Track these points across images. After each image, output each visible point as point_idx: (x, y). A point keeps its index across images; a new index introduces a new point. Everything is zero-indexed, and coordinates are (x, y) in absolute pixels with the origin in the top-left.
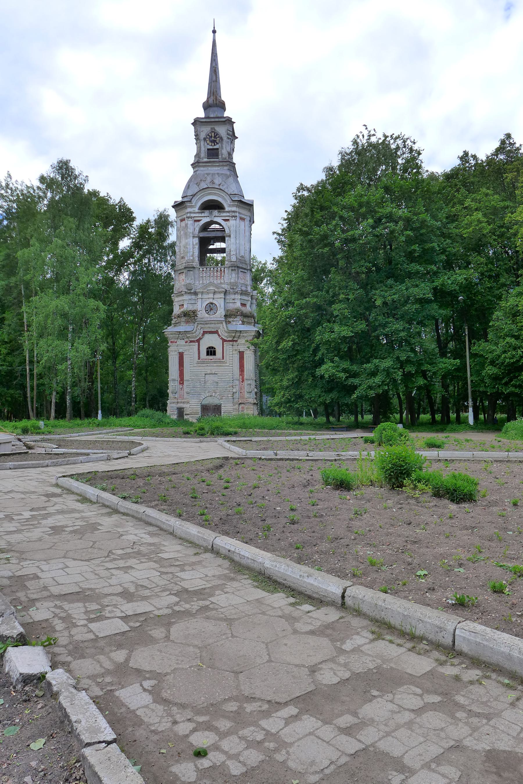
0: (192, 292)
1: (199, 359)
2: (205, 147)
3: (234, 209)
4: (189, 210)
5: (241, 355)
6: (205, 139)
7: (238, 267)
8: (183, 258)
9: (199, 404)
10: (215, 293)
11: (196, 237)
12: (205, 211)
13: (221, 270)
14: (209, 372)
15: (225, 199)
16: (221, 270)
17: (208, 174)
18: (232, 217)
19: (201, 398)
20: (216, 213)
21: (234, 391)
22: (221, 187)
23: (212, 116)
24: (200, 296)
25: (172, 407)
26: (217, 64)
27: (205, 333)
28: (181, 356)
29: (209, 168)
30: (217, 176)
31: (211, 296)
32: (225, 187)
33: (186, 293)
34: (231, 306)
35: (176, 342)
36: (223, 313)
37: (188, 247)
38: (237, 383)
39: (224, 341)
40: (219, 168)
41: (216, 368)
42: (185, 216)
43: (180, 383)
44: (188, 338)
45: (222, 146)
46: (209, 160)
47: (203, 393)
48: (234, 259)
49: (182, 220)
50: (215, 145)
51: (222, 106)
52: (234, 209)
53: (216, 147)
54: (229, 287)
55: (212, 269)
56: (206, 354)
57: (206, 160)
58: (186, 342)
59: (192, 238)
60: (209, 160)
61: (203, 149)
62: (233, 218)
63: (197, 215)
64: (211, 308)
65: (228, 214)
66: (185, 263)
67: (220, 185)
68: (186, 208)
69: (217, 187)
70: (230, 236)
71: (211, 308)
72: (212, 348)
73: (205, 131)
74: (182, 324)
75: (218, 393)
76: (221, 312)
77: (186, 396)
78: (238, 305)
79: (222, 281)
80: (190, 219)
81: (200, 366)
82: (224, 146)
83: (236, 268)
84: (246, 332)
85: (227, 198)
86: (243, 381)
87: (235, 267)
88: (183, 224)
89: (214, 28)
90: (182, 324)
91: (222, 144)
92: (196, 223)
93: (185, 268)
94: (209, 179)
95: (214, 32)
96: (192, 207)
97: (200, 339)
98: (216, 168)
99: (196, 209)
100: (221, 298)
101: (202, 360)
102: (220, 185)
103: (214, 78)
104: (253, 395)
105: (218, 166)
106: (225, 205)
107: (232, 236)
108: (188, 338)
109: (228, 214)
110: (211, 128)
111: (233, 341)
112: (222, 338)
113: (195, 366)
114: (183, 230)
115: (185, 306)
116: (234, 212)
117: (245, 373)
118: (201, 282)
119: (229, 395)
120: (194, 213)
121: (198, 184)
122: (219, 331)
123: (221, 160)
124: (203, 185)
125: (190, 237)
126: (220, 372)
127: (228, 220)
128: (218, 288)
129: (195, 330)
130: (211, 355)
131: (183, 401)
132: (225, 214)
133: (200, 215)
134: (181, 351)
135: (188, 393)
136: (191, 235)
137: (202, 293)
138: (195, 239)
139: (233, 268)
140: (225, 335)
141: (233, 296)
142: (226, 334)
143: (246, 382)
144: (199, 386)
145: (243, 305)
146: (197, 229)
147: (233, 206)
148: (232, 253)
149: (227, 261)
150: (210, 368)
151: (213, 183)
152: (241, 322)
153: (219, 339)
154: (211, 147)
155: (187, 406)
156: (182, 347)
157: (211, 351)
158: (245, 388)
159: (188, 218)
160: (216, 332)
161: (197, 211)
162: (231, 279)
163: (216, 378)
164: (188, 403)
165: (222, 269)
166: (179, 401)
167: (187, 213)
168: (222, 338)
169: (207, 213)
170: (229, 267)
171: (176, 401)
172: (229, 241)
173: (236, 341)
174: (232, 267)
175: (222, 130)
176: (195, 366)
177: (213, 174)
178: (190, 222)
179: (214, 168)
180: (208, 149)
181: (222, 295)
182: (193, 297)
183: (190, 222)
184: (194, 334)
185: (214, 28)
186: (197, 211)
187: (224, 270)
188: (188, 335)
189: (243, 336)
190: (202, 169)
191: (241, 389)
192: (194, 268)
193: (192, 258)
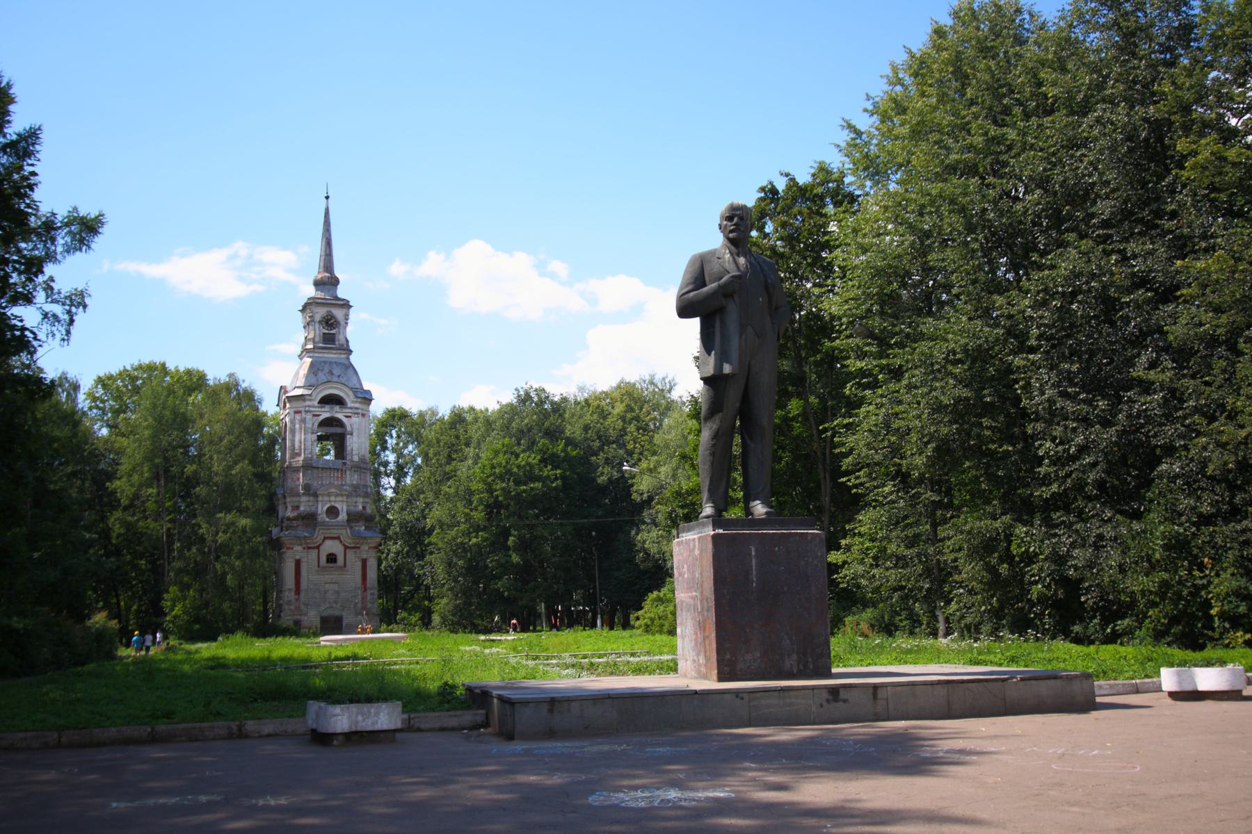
1: (319, 566)
2: (320, 330)
3: (357, 405)
4: (308, 403)
5: (364, 562)
7: (361, 468)
10: (337, 495)
15: (348, 395)
17: (325, 362)
18: (355, 414)
20: (337, 408)
24: (320, 498)
26: (330, 235)
27: (325, 538)
28: (298, 563)
29: (326, 355)
30: (335, 366)
31: (332, 498)
32: (345, 379)
34: (352, 508)
38: (360, 592)
39: (346, 547)
42: (302, 409)
44: (307, 544)
49: (295, 412)
52: (357, 405)
57: (321, 345)
58: (304, 548)
63: (317, 409)
64: (333, 511)
65: (350, 411)
67: (339, 376)
68: (304, 400)
69: (335, 379)
70: (352, 434)
71: (333, 511)
72: (333, 554)
73: (320, 312)
76: (343, 516)
77: (303, 607)
82: (341, 331)
85: (351, 393)
86: (365, 590)
88: (298, 417)
90: (300, 528)
93: (303, 466)
94: (326, 370)
95: (327, 198)
96: (311, 400)
97: (320, 545)
99: (316, 403)
102: (339, 376)
103: (328, 252)
106: (347, 400)
112: (344, 545)
115: (302, 509)
116: (357, 408)
120: (314, 407)
121: (315, 374)
127: (350, 417)
130: (331, 562)
132: (347, 410)
134: (298, 557)
136: (310, 431)
137: (323, 495)
140: (349, 542)
141: (355, 499)
142: (350, 541)
143: (369, 592)
145: (364, 508)
146: (316, 424)
147: (356, 402)
148: (354, 453)
151: (332, 374)
154: (327, 332)
157: (332, 558)
158: (369, 598)
159: (306, 412)
160: (338, 538)
163: (336, 587)
168: (344, 545)
169: (327, 408)
173: (359, 548)
175: (338, 313)
177: (331, 363)
178: (309, 416)
180: (324, 334)
181: (345, 499)
182: (312, 498)
183: (309, 416)
190: (316, 355)
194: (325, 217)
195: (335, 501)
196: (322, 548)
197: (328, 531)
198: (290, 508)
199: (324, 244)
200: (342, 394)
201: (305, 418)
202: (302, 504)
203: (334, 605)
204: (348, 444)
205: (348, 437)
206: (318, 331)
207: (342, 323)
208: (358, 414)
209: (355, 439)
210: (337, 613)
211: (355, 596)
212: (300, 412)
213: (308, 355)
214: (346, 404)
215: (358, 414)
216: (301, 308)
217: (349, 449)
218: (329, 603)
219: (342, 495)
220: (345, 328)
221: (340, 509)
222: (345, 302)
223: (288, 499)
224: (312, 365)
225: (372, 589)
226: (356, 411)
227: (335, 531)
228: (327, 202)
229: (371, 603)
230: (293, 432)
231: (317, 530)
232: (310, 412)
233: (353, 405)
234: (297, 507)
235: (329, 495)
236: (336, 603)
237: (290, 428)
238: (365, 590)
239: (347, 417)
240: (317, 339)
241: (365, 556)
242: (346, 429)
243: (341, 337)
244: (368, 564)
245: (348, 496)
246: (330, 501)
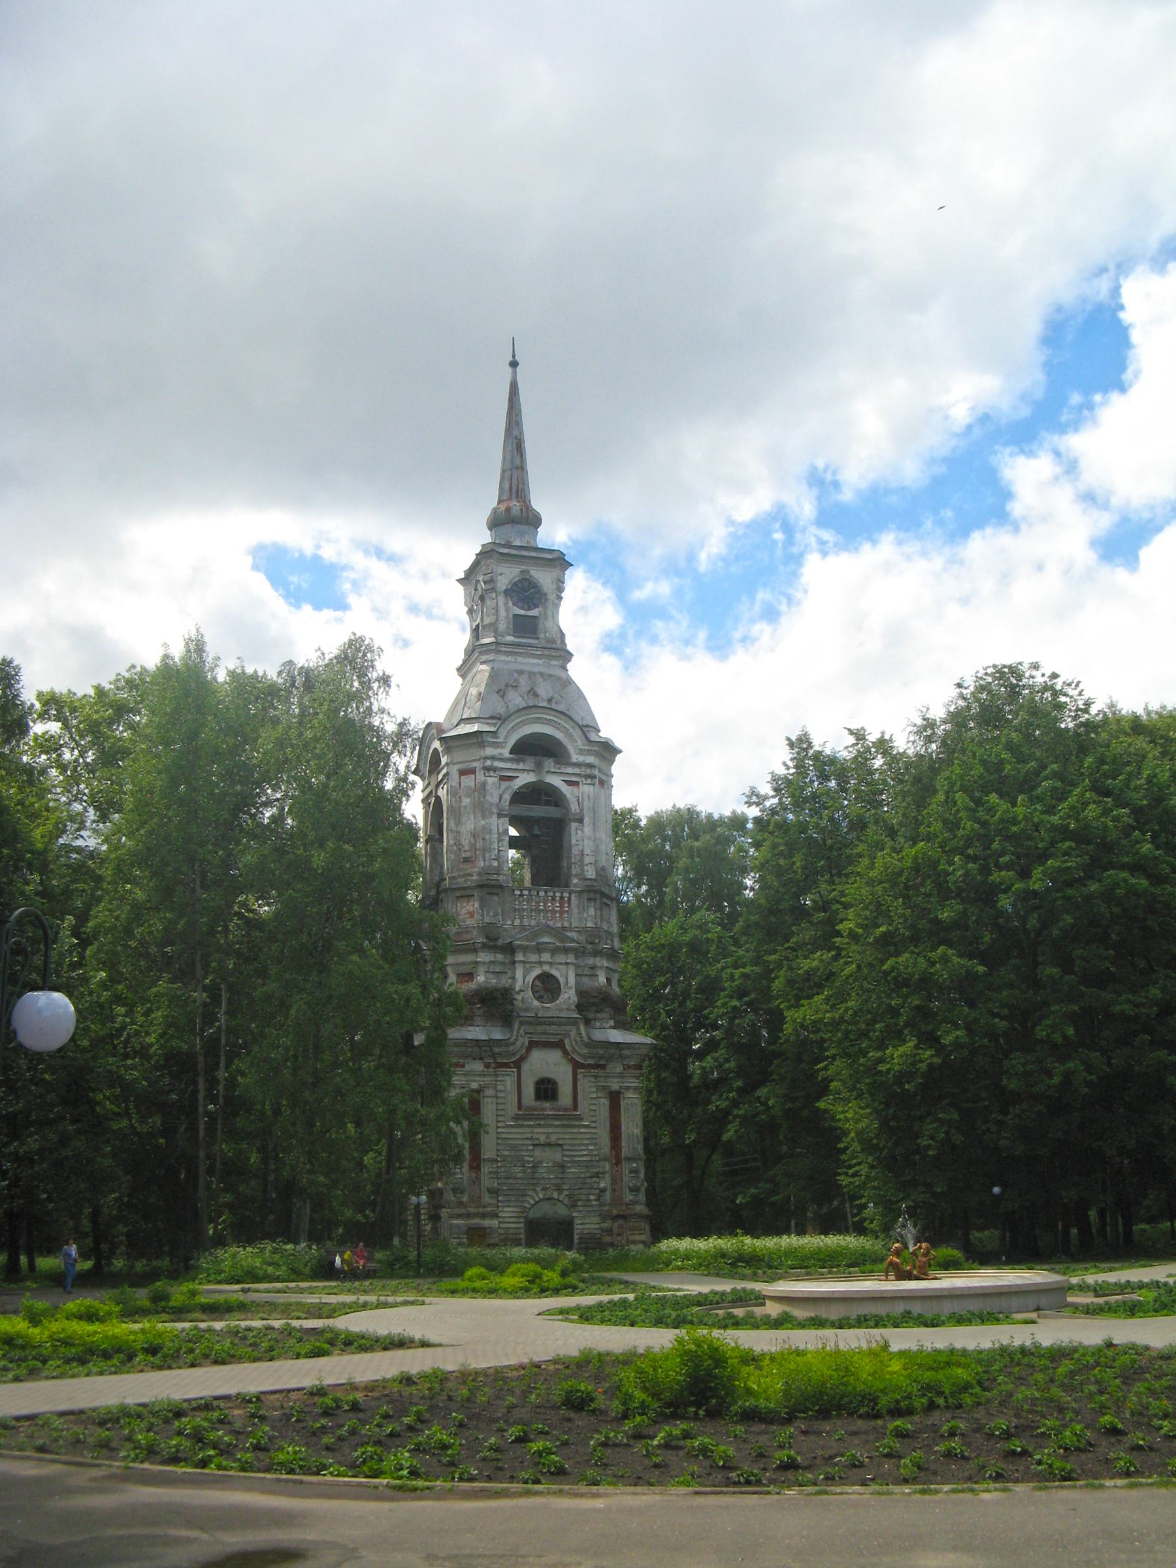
0: (494, 941)
1: (520, 1107)
2: (507, 610)
4: (490, 751)
5: (615, 1098)
6: (506, 592)
8: (466, 860)
9: (523, 1220)
10: (555, 951)
11: (506, 816)
12: (526, 757)
13: (562, 898)
14: (543, 1139)
16: (562, 898)
17: (520, 672)
19: (527, 1205)
20: (549, 764)
21: (602, 1185)
22: (554, 706)
23: (517, 543)
24: (519, 957)
25: (458, 1227)
26: (521, 433)
27: (533, 1045)
29: (519, 659)
31: (546, 957)
33: (485, 946)
35: (463, 1066)
36: (575, 999)
37: (487, 837)
38: (607, 1166)
39: (576, 1065)
40: (541, 662)
41: (559, 1130)
42: (475, 764)
43: (471, 1168)
44: (493, 1055)
45: (546, 613)
46: (517, 640)
47: (530, 1193)
48: (591, 873)
49: (462, 773)
50: (530, 609)
51: (533, 521)
52: (590, 759)
53: (534, 613)
54: (582, 938)
55: (542, 894)
56: (533, 1096)
57: (510, 639)
58: (487, 1066)
59: (495, 817)
60: (517, 640)
61: (502, 613)
62: (589, 781)
63: (508, 765)
64: (548, 986)
65: (577, 771)
66: (480, 874)
67: (550, 701)
68: (482, 745)
69: (545, 704)
70: (580, 821)
71: (548, 986)
73: (507, 575)
74: (478, 1020)
75: (566, 1193)
76: (569, 996)
78: (602, 979)
79: (566, 924)
80: (492, 773)
81: (522, 1126)
82: (549, 613)
83: (598, 896)
84: (630, 1045)
85: (577, 733)
86: (618, 1162)
87: (595, 892)
88: (468, 781)
89: (514, 356)
90: (478, 1020)
91: (545, 608)
92: (505, 784)
93: (481, 886)
95: (514, 364)
96: (496, 745)
97: (522, 1059)
98: (535, 661)
99: (505, 752)
100: (567, 963)
101: (528, 1109)
104: (642, 1197)
105: (539, 657)
107: (587, 820)
108: (493, 1055)
109: (577, 771)
110: (522, 572)
111: (597, 1066)
113: (511, 1126)
114: (468, 796)
115: (481, 978)
116: (591, 766)
117: (623, 1144)
118: (517, 922)
119: (592, 1197)
120: (502, 760)
121: (501, 693)
122: (567, 1041)
123: (543, 643)
124: (516, 699)
125: (491, 813)
126: (569, 1142)
128: (562, 941)
129: (514, 1037)
131: (481, 1210)
132: (570, 770)
133: (514, 766)
135: (494, 1192)
137: (525, 949)
138: (502, 820)
139: (592, 895)
141: (591, 961)
142: (585, 1051)
143: (625, 1168)
144: (520, 1175)
146: (507, 797)
147: (589, 752)
148: (587, 860)
149: (577, 876)
150: (545, 1130)
151: (536, 695)
152: (612, 1023)
153: (564, 1061)
154: (522, 612)
155: (494, 1223)
156: (478, 1079)
157: (546, 1089)
159: (487, 769)
160: (559, 1045)
161: (507, 755)
163: (558, 1156)
164: (495, 1215)
165: (566, 895)
166: (472, 1210)
167: (486, 758)
169: (529, 763)
170: (582, 892)
171: (463, 1211)
172: (579, 832)
173: (603, 1067)
174: (589, 891)
175: (543, 577)
176: (511, 1126)
177: (531, 675)
179: (531, 660)
180: (514, 615)
181: (571, 958)
182: (500, 957)
184: (511, 1048)
185: (514, 356)
186: (507, 755)
187: (569, 899)
188: (497, 1050)
189: (621, 1056)
190: (503, 658)
191: (614, 1181)
192: (501, 887)
193: (496, 864)
194: (511, 400)
195: (551, 964)
196: (525, 1067)
197: (539, 1029)
198: (452, 978)
199: (509, 448)
200: (558, 735)
201: (484, 784)
202: (482, 969)
203: (555, 1195)
204: (573, 842)
205: (574, 825)
206: (505, 610)
207: (552, 597)
208: (592, 777)
209: (587, 830)
210: (562, 1211)
211: (597, 1175)
212: (472, 771)
213: (484, 658)
214: (569, 756)
215: (592, 777)
216: (462, 576)
217: (575, 851)
218: (544, 1189)
219: (566, 951)
220: (557, 607)
221: (562, 981)
222: (555, 555)
223: (451, 959)
224: (494, 676)
225: (629, 1159)
226: (588, 771)
227: (553, 1029)
228: (514, 374)
229: (631, 1190)
230: (456, 812)
231: (516, 1026)
232: (495, 769)
233: (581, 759)
234: (470, 976)
235: (539, 949)
236: (559, 1189)
237: (450, 807)
238: (618, 1162)
239: (569, 783)
240: (502, 626)
241: (615, 1087)
242: (567, 809)
243: (549, 624)
244: (623, 1103)
245: (579, 952)
246: (541, 963)
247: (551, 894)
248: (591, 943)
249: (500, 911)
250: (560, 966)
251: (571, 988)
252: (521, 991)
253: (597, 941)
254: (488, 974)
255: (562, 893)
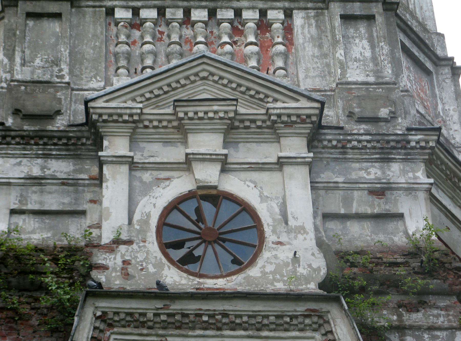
162: (343, 66)
247: (230, 14)
248: (362, 120)
249: (65, 52)
250: (256, 176)
251: (301, 230)
252: (117, 242)
253: (384, 112)
254: (20, 220)
255: (263, 13)
